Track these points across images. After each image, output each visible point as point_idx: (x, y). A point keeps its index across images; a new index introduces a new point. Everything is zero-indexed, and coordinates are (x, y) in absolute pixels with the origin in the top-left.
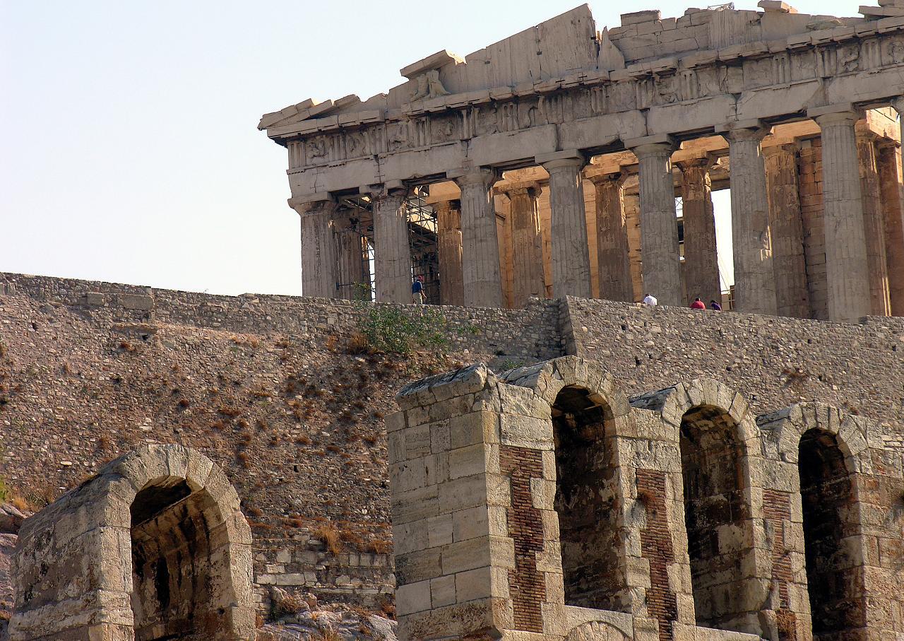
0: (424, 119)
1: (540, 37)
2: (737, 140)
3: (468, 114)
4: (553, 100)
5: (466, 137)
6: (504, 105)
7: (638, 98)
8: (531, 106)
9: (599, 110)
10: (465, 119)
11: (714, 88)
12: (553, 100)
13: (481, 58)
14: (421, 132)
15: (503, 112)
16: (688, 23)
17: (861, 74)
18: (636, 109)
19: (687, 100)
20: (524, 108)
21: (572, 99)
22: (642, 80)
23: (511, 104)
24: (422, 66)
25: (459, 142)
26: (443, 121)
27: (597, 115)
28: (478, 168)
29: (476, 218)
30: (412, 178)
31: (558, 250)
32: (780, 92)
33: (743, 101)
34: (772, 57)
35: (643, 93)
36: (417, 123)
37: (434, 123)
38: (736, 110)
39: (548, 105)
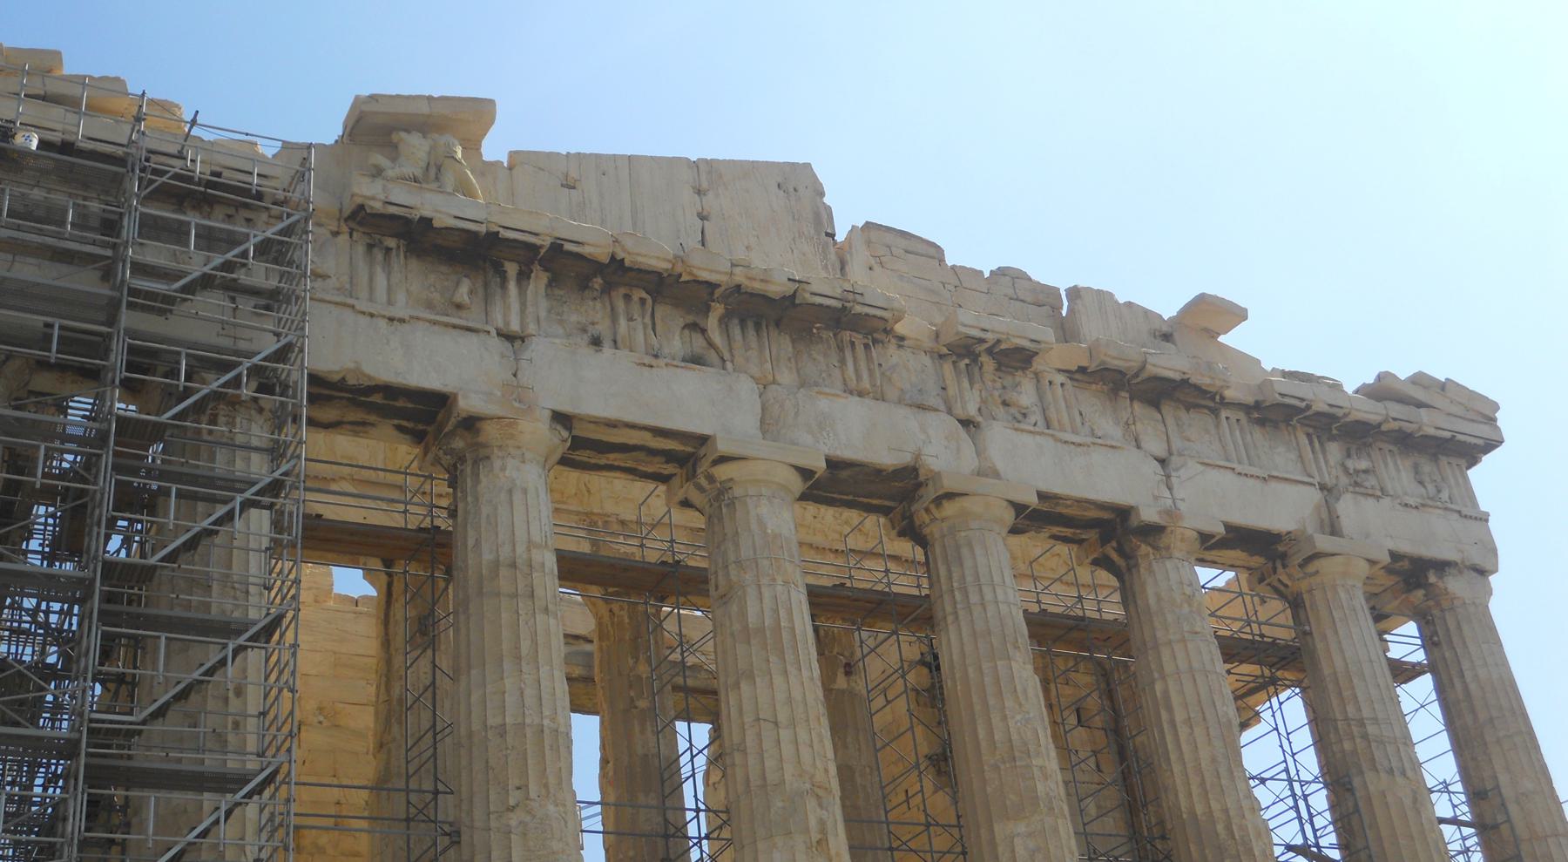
0: (391, 242)
1: (705, 185)
2: (1177, 554)
3: (524, 276)
4: (750, 324)
5: (515, 326)
6: (622, 291)
7: (951, 392)
8: (690, 319)
9: (866, 384)
10: (512, 286)
11: (1108, 426)
12: (750, 324)
13: (570, 174)
14: (379, 270)
15: (620, 305)
16: (1010, 292)
17: (1386, 501)
18: (950, 412)
19: (1062, 429)
20: (671, 319)
21: (793, 341)
22: (961, 356)
23: (644, 295)
24: (424, 109)
25: (494, 333)
26: (444, 268)
27: (861, 394)
28: (547, 414)
29: (530, 544)
30: (336, 378)
31: (780, 696)
32: (1251, 482)
33: (1182, 472)
34: (1215, 412)
35: (966, 384)
36: (370, 247)
37: (414, 264)
38: (1170, 489)
39: (736, 331)
